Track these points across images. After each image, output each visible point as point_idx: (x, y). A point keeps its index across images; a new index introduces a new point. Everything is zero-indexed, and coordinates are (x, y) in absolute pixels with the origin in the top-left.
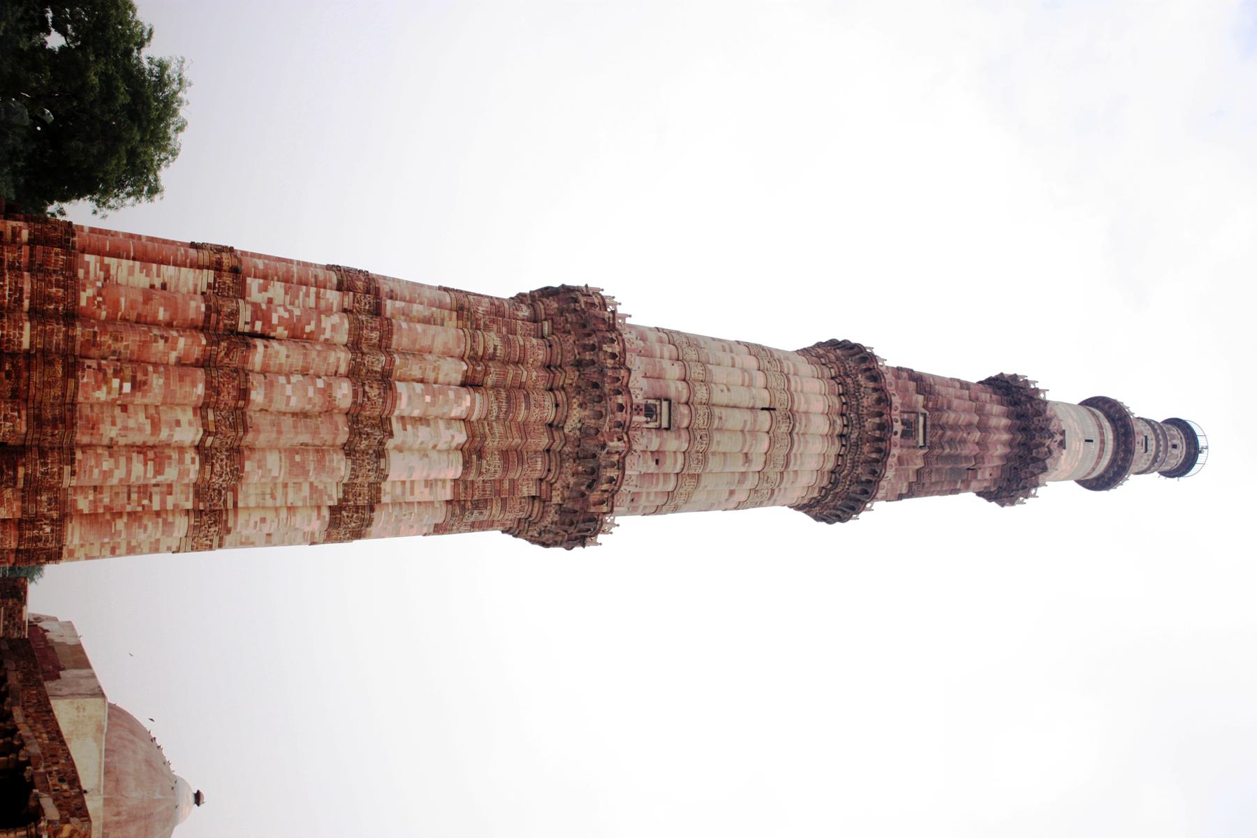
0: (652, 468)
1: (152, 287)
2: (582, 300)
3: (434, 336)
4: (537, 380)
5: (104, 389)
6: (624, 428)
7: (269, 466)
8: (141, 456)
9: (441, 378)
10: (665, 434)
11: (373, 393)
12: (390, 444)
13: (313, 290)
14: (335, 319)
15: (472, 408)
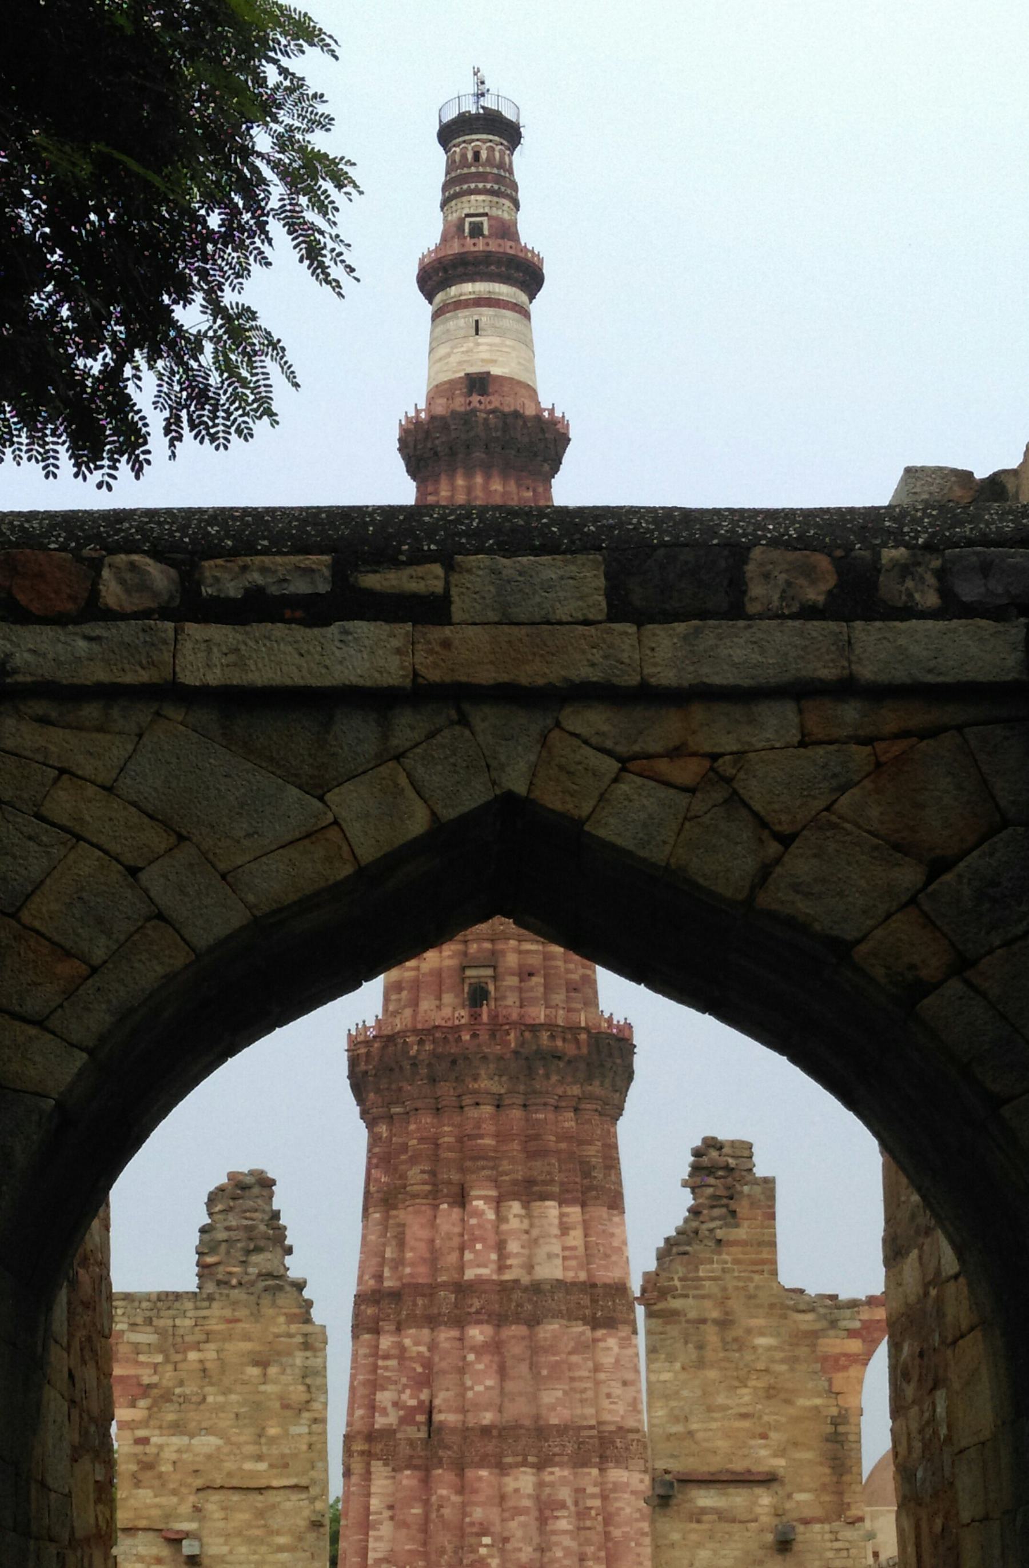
0: (537, 980)
1: (392, 1518)
2: (363, 1067)
3: (416, 1239)
4: (453, 1125)
5: (489, 1560)
6: (497, 1028)
7: (554, 1401)
8: (550, 1522)
9: (457, 1230)
10: (500, 970)
11: (477, 1304)
12: (525, 1280)
13: (380, 1363)
14: (407, 1342)
15: (485, 1198)
